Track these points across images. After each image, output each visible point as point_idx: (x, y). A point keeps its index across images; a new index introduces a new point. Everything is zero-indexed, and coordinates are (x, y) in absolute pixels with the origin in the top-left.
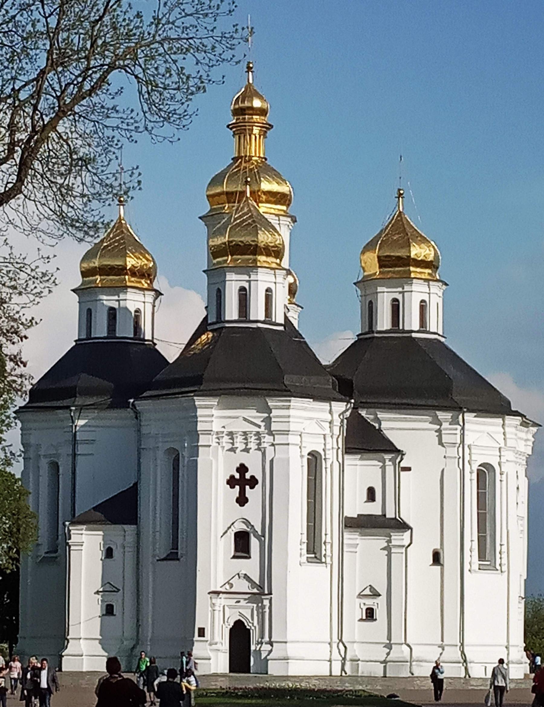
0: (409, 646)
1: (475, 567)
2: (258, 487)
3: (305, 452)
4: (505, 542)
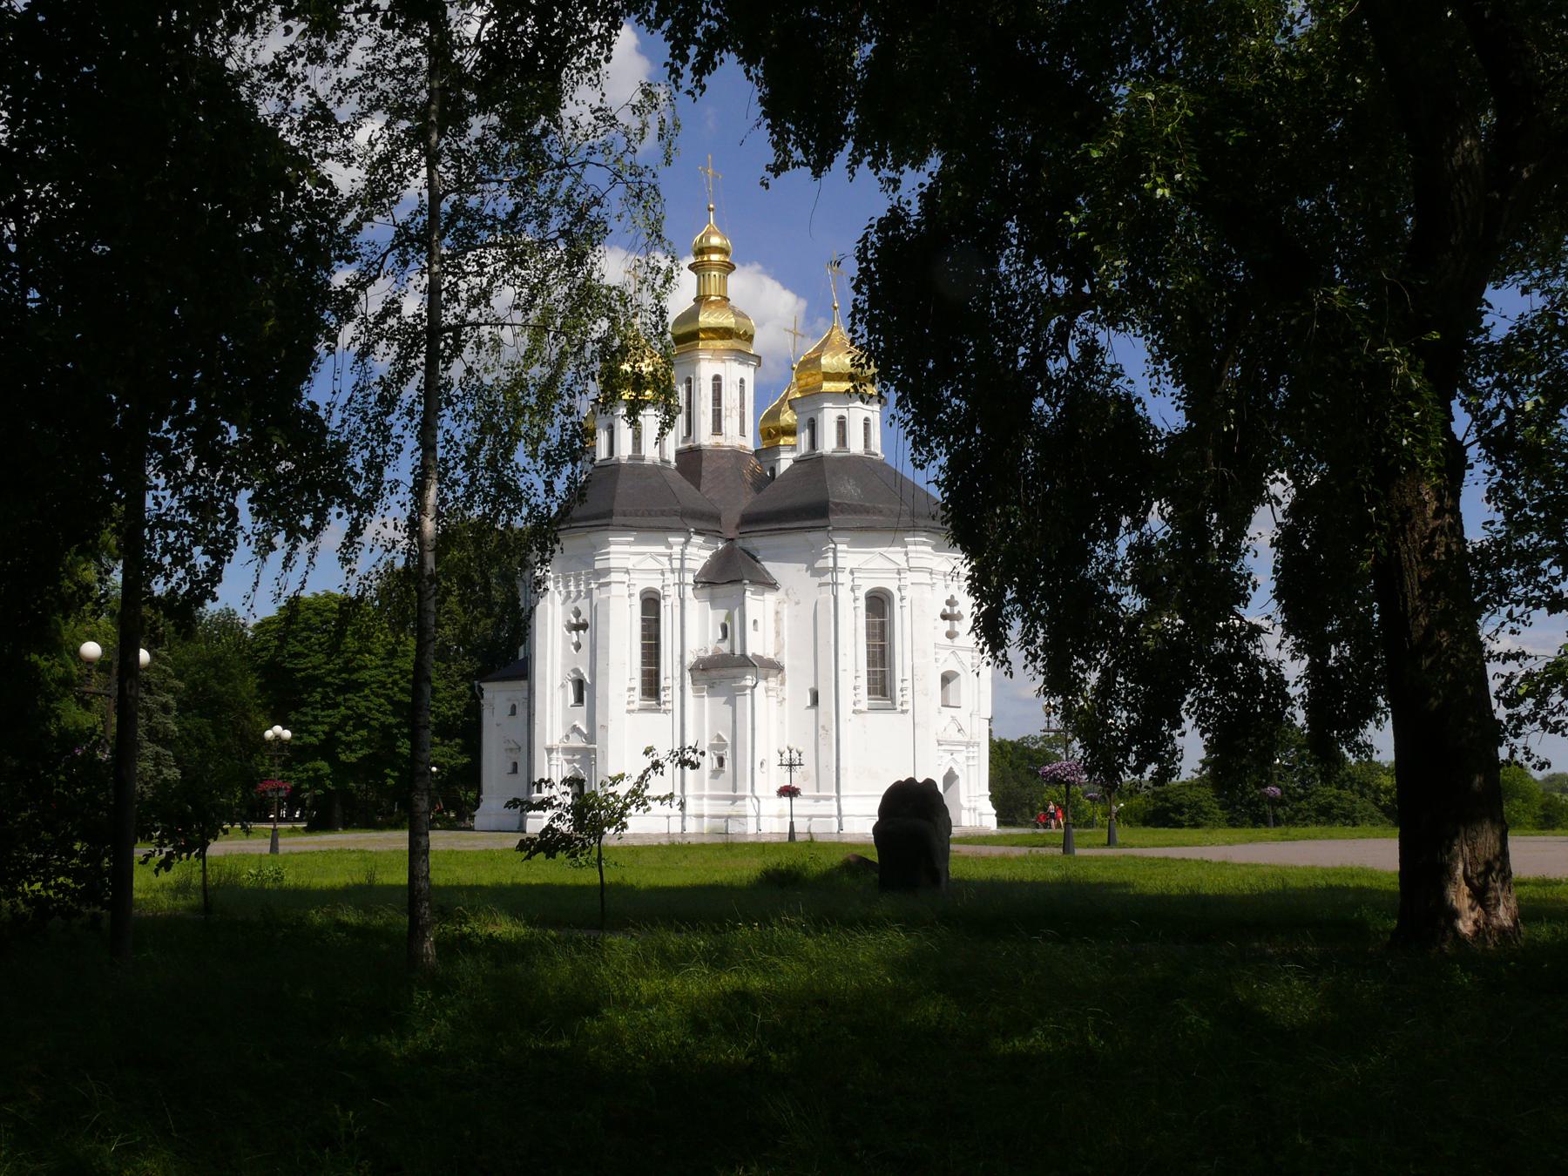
0: (757, 798)
1: (864, 705)
2: (588, 630)
3: (637, 592)
4: (908, 675)
